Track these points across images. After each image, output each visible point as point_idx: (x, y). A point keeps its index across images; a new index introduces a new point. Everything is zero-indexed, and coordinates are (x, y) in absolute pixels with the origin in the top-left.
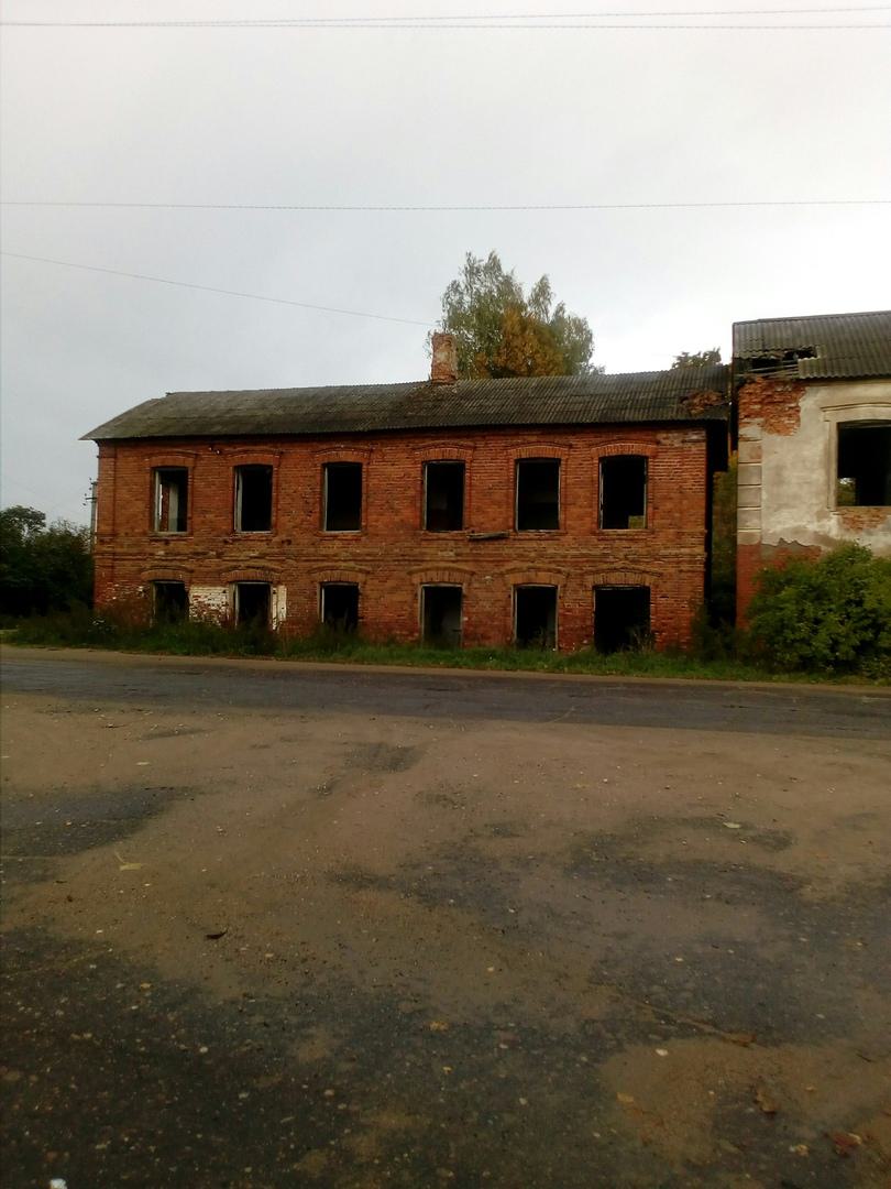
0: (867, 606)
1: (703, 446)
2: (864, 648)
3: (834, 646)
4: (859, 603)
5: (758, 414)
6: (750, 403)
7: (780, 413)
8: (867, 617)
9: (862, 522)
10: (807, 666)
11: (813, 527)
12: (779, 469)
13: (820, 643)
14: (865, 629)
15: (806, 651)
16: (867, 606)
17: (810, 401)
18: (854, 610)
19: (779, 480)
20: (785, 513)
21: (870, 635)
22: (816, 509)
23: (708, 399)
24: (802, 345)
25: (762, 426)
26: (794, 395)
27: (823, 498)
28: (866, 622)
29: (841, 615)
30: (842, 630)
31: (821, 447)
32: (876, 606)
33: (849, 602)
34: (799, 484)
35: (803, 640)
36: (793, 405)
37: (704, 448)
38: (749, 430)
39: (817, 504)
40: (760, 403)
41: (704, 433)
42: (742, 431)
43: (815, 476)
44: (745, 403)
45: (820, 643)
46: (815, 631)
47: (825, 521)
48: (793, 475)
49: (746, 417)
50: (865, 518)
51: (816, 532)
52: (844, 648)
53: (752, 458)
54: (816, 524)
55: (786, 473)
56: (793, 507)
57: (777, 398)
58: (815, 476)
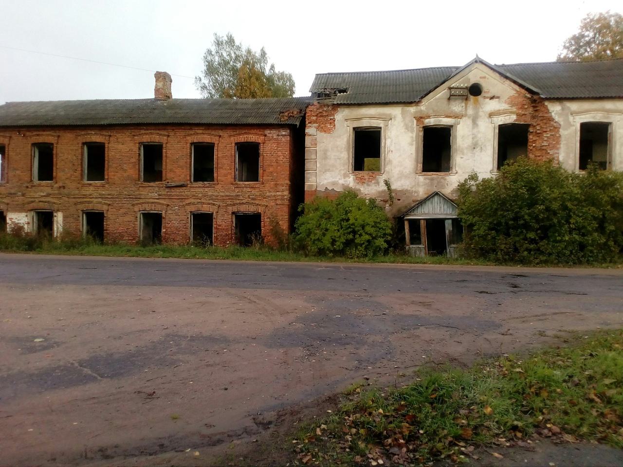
0: (351, 222)
1: (288, 138)
2: (349, 243)
3: (333, 242)
4: (348, 220)
5: (315, 122)
6: (311, 115)
7: (326, 124)
8: (350, 227)
9: (365, 179)
10: (321, 253)
11: (341, 182)
12: (325, 151)
13: (326, 242)
14: (349, 233)
15: (320, 245)
16: (351, 222)
17: (341, 116)
18: (344, 224)
19: (325, 158)
20: (328, 174)
21: (351, 236)
22: (343, 172)
23: (292, 113)
24: (343, 87)
25: (317, 128)
26: (333, 112)
27: (346, 167)
28: (350, 230)
29: (338, 226)
30: (337, 234)
31: (345, 140)
32: (354, 221)
33: (343, 220)
34: (335, 159)
35: (318, 240)
36: (332, 118)
37: (289, 139)
38: (310, 130)
39: (343, 170)
40: (316, 116)
41: (288, 131)
42: (307, 131)
43: (342, 155)
44: (308, 116)
45: (326, 242)
46: (324, 235)
47: (347, 179)
48: (332, 155)
49: (309, 123)
50: (366, 177)
51: (343, 184)
52: (338, 244)
53: (312, 145)
54: (343, 180)
55: (329, 154)
56: (333, 171)
57: (325, 114)
58: (342, 155)
